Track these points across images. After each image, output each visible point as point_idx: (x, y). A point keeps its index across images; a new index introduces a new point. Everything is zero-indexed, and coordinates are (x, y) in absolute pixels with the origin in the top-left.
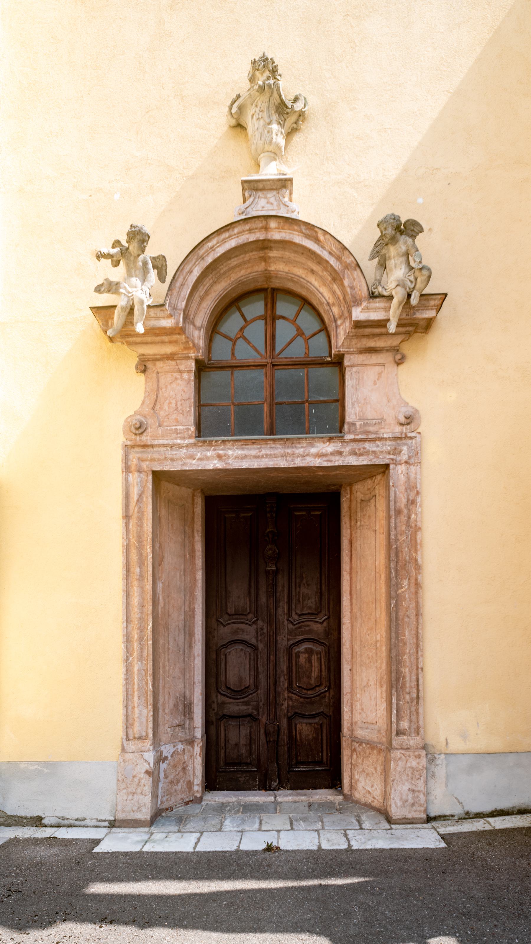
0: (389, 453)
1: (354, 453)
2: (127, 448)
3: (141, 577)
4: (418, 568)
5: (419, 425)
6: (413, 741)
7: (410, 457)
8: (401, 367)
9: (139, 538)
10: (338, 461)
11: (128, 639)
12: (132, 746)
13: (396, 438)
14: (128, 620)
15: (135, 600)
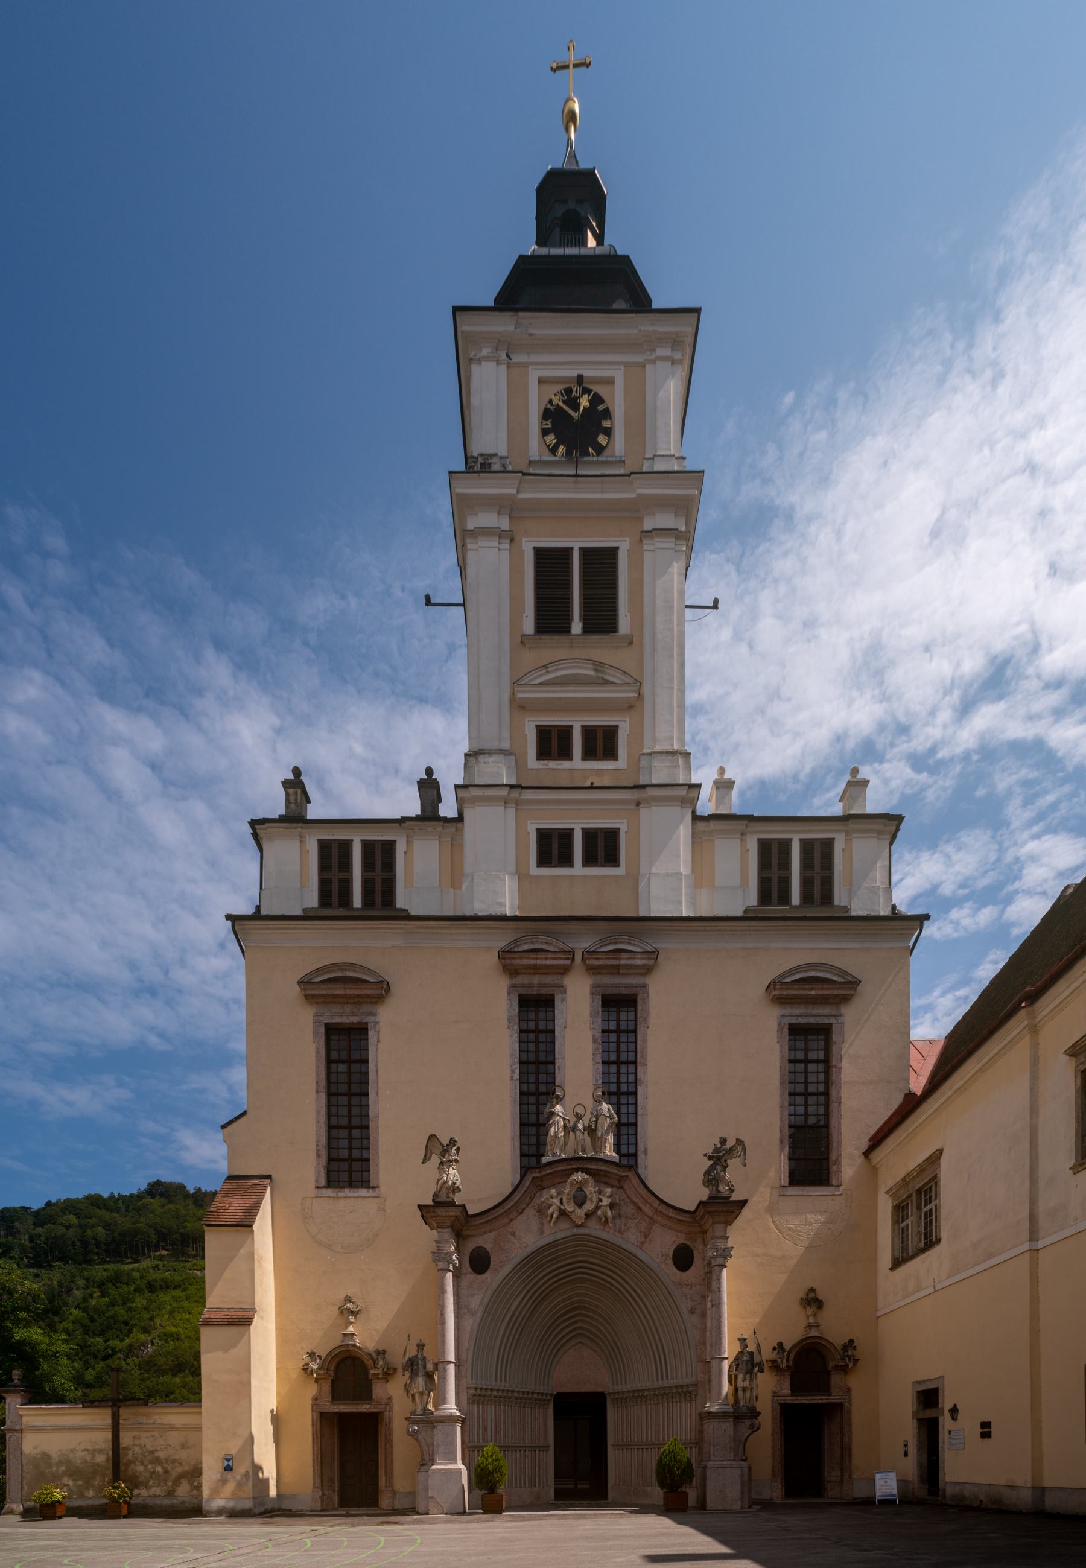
2: (312, 1405)
3: (317, 1443)
4: (392, 1441)
6: (390, 1489)
9: (317, 1431)
11: (314, 1460)
12: (315, 1490)
14: (314, 1454)
15: (316, 1449)
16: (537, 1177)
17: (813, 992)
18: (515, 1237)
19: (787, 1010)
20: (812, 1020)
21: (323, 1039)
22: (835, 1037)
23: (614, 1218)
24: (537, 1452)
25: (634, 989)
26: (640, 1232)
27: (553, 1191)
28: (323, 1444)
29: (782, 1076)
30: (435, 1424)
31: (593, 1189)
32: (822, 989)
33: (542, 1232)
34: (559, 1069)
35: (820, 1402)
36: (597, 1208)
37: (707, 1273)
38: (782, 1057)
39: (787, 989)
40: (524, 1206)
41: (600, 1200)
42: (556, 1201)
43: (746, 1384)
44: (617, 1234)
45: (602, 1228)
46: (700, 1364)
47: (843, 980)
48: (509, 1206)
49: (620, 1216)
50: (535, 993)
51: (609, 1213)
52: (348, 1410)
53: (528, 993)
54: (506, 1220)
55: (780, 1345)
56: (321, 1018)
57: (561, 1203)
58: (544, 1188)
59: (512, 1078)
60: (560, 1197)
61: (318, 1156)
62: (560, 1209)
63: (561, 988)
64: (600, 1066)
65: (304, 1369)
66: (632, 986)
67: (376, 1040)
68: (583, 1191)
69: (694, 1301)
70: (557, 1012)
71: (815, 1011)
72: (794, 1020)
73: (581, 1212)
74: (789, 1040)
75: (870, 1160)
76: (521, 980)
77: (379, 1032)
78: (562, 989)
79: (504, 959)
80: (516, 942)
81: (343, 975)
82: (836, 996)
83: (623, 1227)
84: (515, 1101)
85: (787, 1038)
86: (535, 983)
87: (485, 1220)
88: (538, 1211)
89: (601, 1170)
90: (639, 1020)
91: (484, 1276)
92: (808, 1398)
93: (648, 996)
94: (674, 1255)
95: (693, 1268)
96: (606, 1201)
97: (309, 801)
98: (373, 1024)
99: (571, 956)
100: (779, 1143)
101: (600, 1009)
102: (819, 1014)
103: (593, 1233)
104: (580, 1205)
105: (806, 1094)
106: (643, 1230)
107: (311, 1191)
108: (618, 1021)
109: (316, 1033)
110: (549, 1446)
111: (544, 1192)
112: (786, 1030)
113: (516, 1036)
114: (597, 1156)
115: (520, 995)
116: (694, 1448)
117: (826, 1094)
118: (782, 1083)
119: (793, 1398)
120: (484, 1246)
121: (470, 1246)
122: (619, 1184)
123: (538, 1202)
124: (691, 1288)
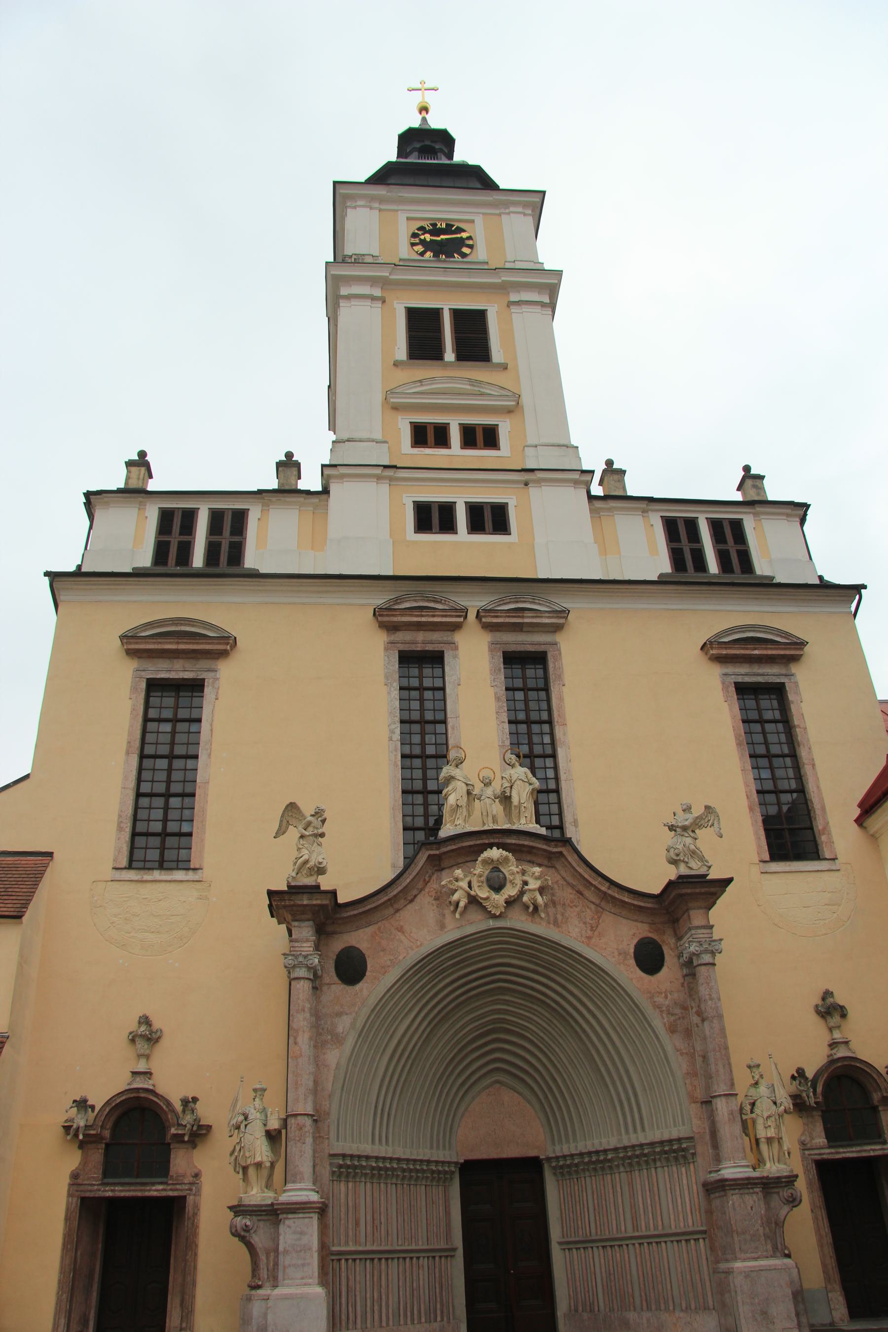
0: (187, 1190)
1: (171, 1190)
5: (200, 1178)
7: (196, 1192)
8: (195, 1150)
10: (164, 1194)
13: (190, 1184)
16: (434, 855)
17: (756, 652)
18: (403, 933)
19: (730, 669)
20: (760, 679)
21: (142, 695)
22: (791, 697)
23: (546, 905)
24: (437, 1258)
25: (543, 646)
26: (585, 923)
27: (458, 872)
28: (79, 1253)
29: (737, 737)
30: (281, 1217)
31: (514, 869)
32: (766, 649)
33: (442, 926)
34: (453, 728)
35: (872, 1154)
36: (522, 893)
37: (686, 975)
38: (733, 717)
39: (726, 648)
40: (415, 892)
41: (526, 883)
42: (464, 884)
43: (771, 1133)
44: (552, 926)
45: (530, 919)
46: (693, 1105)
47: (787, 641)
48: (395, 892)
49: (554, 903)
50: (418, 649)
51: (540, 900)
52: (127, 1194)
53: (410, 649)
54: (391, 910)
55: (801, 1072)
56: (143, 673)
57: (470, 886)
58: (443, 869)
59: (391, 739)
60: (467, 879)
61: (120, 829)
62: (469, 895)
63: (452, 645)
64: (506, 725)
65: (64, 1127)
66: (540, 644)
67: (214, 697)
68: (500, 871)
69: (672, 1015)
70: (447, 669)
71: (761, 671)
72: (740, 679)
73: (499, 899)
74: (738, 699)
75: (865, 828)
76: (400, 636)
77: (218, 688)
78: (454, 646)
79: (380, 615)
80: (397, 601)
81: (177, 629)
82: (783, 656)
83: (559, 917)
84: (395, 764)
85: (735, 697)
86: (421, 641)
87: (361, 910)
88: (436, 899)
89: (523, 846)
90: (552, 677)
91: (358, 987)
92: (854, 1149)
93: (560, 654)
94: (635, 953)
95: (664, 971)
96: (534, 884)
97: (151, 477)
98: (211, 680)
99: (464, 614)
100: (748, 810)
101: (502, 666)
102: (769, 674)
103: (518, 925)
104: (497, 888)
105: (769, 756)
106: (588, 920)
107: (110, 874)
108: (524, 678)
109: (134, 689)
110: (454, 1250)
111: (444, 873)
112: (732, 689)
113: (396, 693)
114: (514, 827)
115: (400, 652)
116: (701, 1241)
117: (794, 755)
118: (739, 744)
119: (833, 1150)
120: (357, 946)
121: (338, 945)
122: (550, 860)
123: (435, 886)
124: (666, 997)
